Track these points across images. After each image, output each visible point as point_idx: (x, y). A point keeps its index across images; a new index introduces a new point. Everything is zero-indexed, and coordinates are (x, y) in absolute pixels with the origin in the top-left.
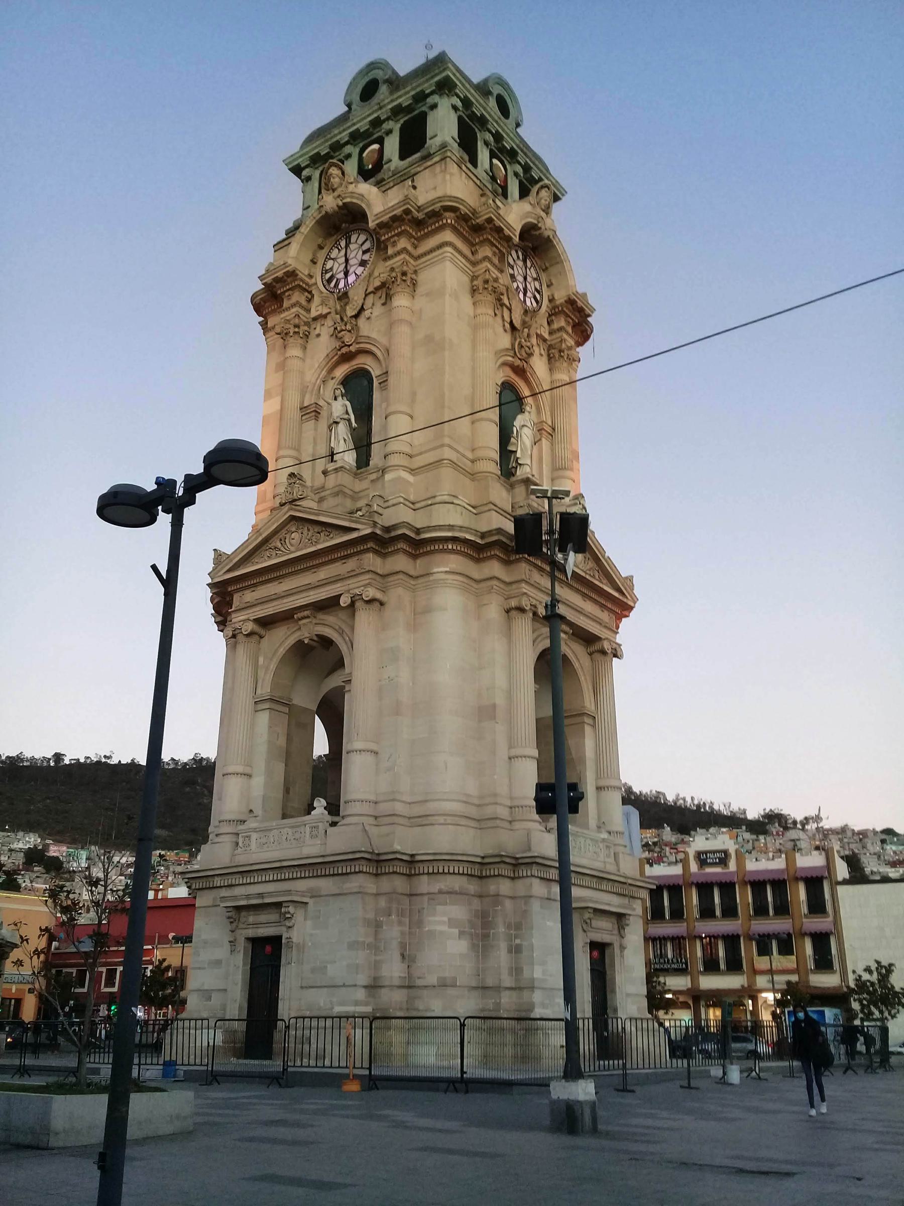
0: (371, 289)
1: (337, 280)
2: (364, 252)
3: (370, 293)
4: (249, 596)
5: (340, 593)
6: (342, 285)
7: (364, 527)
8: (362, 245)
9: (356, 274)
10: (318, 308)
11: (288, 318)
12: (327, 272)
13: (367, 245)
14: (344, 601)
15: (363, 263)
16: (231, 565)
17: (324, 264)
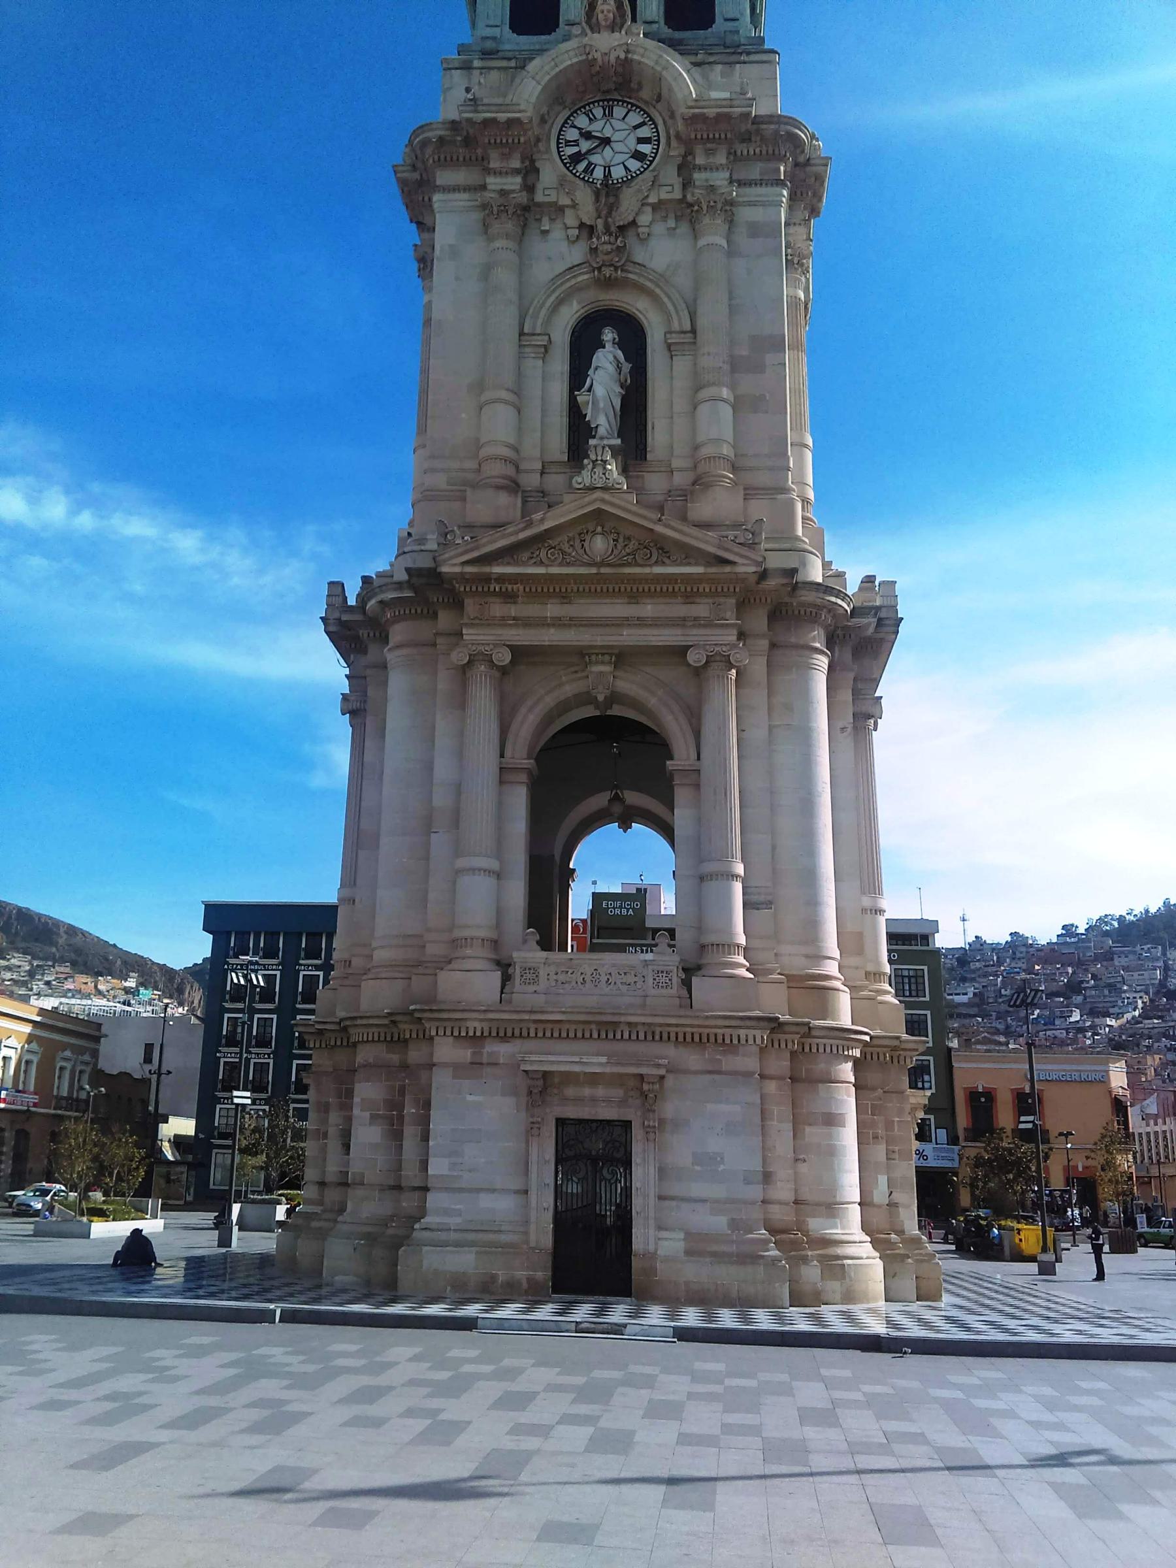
0: (651, 200)
1: (590, 164)
2: (641, 141)
3: (648, 204)
4: (498, 609)
5: (691, 644)
6: (599, 173)
8: (636, 127)
9: (626, 168)
13: (645, 132)
14: (693, 658)
15: (638, 156)
16: (475, 554)
17: (561, 130)
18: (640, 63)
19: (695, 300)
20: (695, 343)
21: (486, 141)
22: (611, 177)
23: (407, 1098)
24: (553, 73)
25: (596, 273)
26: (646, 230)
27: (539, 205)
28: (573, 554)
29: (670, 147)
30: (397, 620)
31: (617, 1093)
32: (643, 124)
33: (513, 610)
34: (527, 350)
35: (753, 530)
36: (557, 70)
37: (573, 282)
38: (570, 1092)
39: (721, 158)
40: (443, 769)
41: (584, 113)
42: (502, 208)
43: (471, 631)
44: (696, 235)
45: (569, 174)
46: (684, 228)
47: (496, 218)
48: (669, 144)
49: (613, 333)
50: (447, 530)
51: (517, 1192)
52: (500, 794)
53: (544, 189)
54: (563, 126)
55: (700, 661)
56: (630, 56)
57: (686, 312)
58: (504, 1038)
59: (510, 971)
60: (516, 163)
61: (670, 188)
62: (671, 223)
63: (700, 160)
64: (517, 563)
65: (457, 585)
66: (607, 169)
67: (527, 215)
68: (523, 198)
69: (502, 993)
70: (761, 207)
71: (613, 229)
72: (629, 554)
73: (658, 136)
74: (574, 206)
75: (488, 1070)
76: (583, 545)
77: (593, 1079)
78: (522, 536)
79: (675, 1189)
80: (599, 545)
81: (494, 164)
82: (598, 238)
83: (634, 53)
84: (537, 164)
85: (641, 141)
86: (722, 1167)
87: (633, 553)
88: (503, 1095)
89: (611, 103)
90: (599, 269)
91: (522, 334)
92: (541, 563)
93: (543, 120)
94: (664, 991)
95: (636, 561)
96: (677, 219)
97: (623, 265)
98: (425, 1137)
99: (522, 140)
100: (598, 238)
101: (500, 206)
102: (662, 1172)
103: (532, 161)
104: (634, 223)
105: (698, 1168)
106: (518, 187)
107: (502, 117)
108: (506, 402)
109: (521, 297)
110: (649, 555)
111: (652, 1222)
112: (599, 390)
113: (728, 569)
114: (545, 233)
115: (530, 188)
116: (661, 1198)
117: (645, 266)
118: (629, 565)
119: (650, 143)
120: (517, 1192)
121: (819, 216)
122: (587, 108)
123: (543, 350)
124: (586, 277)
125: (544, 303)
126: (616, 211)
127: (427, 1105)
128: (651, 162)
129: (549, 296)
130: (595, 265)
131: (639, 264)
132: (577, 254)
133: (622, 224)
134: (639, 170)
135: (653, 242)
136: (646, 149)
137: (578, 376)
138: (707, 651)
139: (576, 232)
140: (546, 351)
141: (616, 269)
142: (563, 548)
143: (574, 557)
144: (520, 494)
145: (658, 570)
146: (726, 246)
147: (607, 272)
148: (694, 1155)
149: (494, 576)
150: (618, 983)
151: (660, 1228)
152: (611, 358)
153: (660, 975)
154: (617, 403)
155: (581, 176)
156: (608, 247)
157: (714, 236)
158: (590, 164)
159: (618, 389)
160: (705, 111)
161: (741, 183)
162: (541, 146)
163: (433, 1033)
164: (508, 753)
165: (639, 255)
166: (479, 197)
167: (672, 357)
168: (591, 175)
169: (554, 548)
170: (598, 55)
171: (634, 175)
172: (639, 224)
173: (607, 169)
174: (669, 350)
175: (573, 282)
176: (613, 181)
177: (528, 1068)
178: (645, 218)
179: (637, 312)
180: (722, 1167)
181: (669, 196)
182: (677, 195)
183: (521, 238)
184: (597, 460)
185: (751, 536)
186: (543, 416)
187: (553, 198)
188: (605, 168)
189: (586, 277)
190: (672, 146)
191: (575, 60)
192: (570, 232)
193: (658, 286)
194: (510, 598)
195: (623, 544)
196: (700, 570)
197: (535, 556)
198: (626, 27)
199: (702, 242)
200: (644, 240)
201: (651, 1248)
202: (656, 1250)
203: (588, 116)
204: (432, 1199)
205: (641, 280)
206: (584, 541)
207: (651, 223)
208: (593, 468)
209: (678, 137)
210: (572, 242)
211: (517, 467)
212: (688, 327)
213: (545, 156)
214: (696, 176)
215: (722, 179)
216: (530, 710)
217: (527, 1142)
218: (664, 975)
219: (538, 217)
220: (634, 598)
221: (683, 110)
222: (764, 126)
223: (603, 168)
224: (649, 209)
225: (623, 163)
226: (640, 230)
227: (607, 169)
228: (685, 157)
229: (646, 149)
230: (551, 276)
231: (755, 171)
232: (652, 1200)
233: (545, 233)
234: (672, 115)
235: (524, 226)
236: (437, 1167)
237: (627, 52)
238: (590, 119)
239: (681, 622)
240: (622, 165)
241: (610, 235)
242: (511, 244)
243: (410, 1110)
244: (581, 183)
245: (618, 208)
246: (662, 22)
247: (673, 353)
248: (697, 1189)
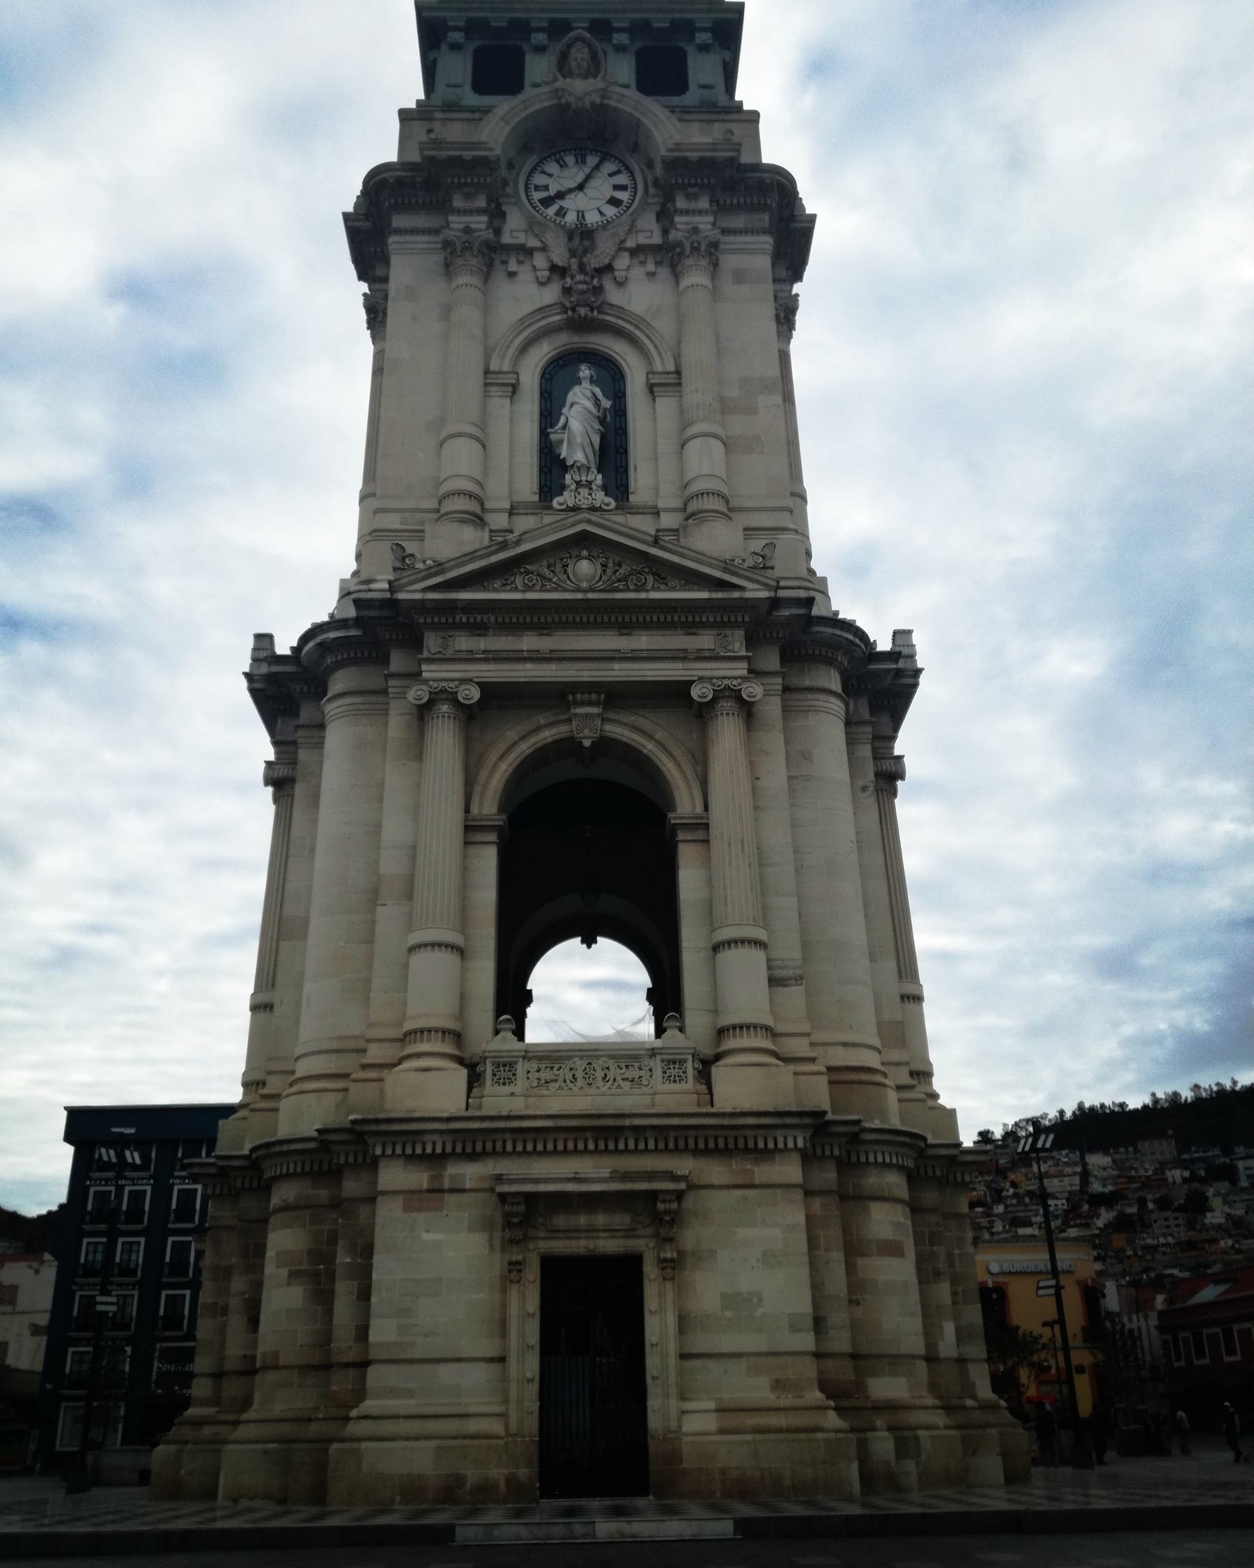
0: (630, 243)
1: (561, 208)
2: (616, 188)
3: (626, 249)
4: (463, 642)
6: (571, 218)
7: (757, 586)
8: (611, 175)
9: (601, 213)
10: (515, 234)
11: (473, 226)
12: (537, 188)
15: (614, 202)
18: (616, 109)
19: (679, 343)
20: (680, 384)
21: (449, 181)
23: (341, 1242)
24: (523, 115)
25: (570, 312)
26: (623, 274)
27: (509, 249)
28: (554, 580)
29: (647, 195)
30: (339, 665)
31: (621, 1220)
32: (618, 172)
33: (482, 644)
34: (493, 389)
35: (762, 553)
36: (528, 112)
37: (543, 323)
38: (561, 1221)
39: (704, 203)
40: (395, 830)
41: (555, 160)
42: (467, 245)
43: (433, 667)
44: (677, 277)
45: (540, 216)
46: (664, 272)
47: (460, 256)
48: (646, 191)
49: (590, 369)
50: (405, 554)
51: (491, 1360)
52: (465, 856)
53: (511, 231)
55: (707, 696)
56: (606, 102)
57: (669, 354)
58: (473, 1157)
59: (479, 1069)
60: (481, 202)
61: (649, 234)
62: (651, 267)
63: (681, 203)
64: (486, 589)
65: (416, 617)
66: (581, 215)
67: (493, 255)
68: (489, 235)
69: (468, 1097)
70: (747, 256)
71: (588, 269)
72: (619, 580)
73: (635, 183)
74: (544, 249)
75: (449, 1198)
76: (566, 571)
77: (592, 1201)
78: (494, 559)
79: (701, 1343)
80: (585, 567)
81: (458, 202)
82: (572, 277)
83: (610, 98)
84: (504, 208)
85: (616, 188)
86: (760, 1312)
87: (624, 579)
88: (471, 1229)
89: (583, 152)
90: (573, 309)
91: (487, 372)
92: (516, 590)
93: (511, 166)
94: (677, 1087)
95: (628, 587)
96: (658, 263)
97: (600, 306)
98: (365, 1294)
99: (489, 180)
100: (572, 277)
101: (464, 243)
102: (684, 1323)
103: (499, 205)
104: (609, 268)
105: (728, 1314)
106: (483, 226)
107: (468, 154)
108: (471, 436)
109: (486, 336)
110: (643, 581)
111: (673, 1391)
112: (576, 425)
113: (736, 595)
114: (512, 275)
115: (498, 232)
116: (684, 1356)
117: (623, 308)
118: (617, 590)
120: (491, 1360)
121: (802, 281)
122: (558, 156)
123: (510, 389)
124: (558, 318)
125: (512, 342)
126: (591, 253)
127: (368, 1251)
128: (628, 208)
129: (517, 335)
130: (568, 304)
131: (616, 306)
132: (551, 294)
133: (597, 266)
134: (615, 215)
135: (632, 286)
136: (624, 196)
137: (549, 413)
138: (714, 685)
139: (546, 274)
140: (514, 392)
141: (592, 309)
142: (542, 573)
143: (555, 583)
144: (487, 529)
145: (655, 595)
146: (710, 286)
147: (582, 311)
148: (724, 1296)
149: (459, 605)
150: (619, 1079)
151: (683, 1398)
152: (590, 395)
153: (672, 1066)
154: (596, 440)
155: (553, 220)
156: (584, 287)
157: (696, 277)
158: (561, 208)
159: (597, 426)
160: (688, 154)
161: (725, 231)
162: (509, 190)
163: (378, 1151)
164: (475, 810)
165: (614, 295)
166: (439, 238)
167: (654, 400)
169: (533, 574)
170: (572, 100)
171: (610, 220)
172: (616, 268)
174: (652, 392)
175: (543, 323)
177: (506, 1188)
178: (622, 262)
179: (614, 355)
180: (760, 1312)
181: (648, 242)
182: (657, 239)
183: (487, 274)
184: (581, 481)
185: (761, 559)
186: (511, 457)
187: (521, 239)
188: (578, 212)
189: (558, 318)
190: (650, 194)
191: (546, 104)
192: (539, 274)
193: (637, 327)
194: (479, 629)
195: (612, 570)
196: (705, 595)
197: (509, 582)
198: (600, 75)
199: (685, 283)
200: (620, 284)
201: (673, 1424)
202: (680, 1427)
203: (558, 162)
204: (374, 1375)
205: (620, 322)
206: (567, 566)
207: (629, 267)
208: (577, 488)
209: (656, 183)
210: (542, 284)
211: (482, 504)
212: (671, 367)
213: (512, 200)
214: (677, 219)
215: (706, 223)
216: (502, 757)
217: (504, 1291)
218: (677, 1066)
219: (504, 258)
220: (626, 628)
221: (663, 152)
222: (749, 175)
224: (626, 255)
226: (617, 273)
227: (580, 214)
228: (663, 205)
229: (624, 196)
230: (519, 317)
231: (739, 221)
232: (673, 1361)
233: (512, 275)
234: (650, 165)
235: (490, 266)
236: (382, 1332)
237: (603, 97)
238: (561, 166)
239: (682, 656)
241: (586, 274)
242: (475, 280)
243: (344, 1258)
244: (553, 225)
245: (593, 250)
246: (634, 86)
247: (656, 394)
248: (727, 1343)
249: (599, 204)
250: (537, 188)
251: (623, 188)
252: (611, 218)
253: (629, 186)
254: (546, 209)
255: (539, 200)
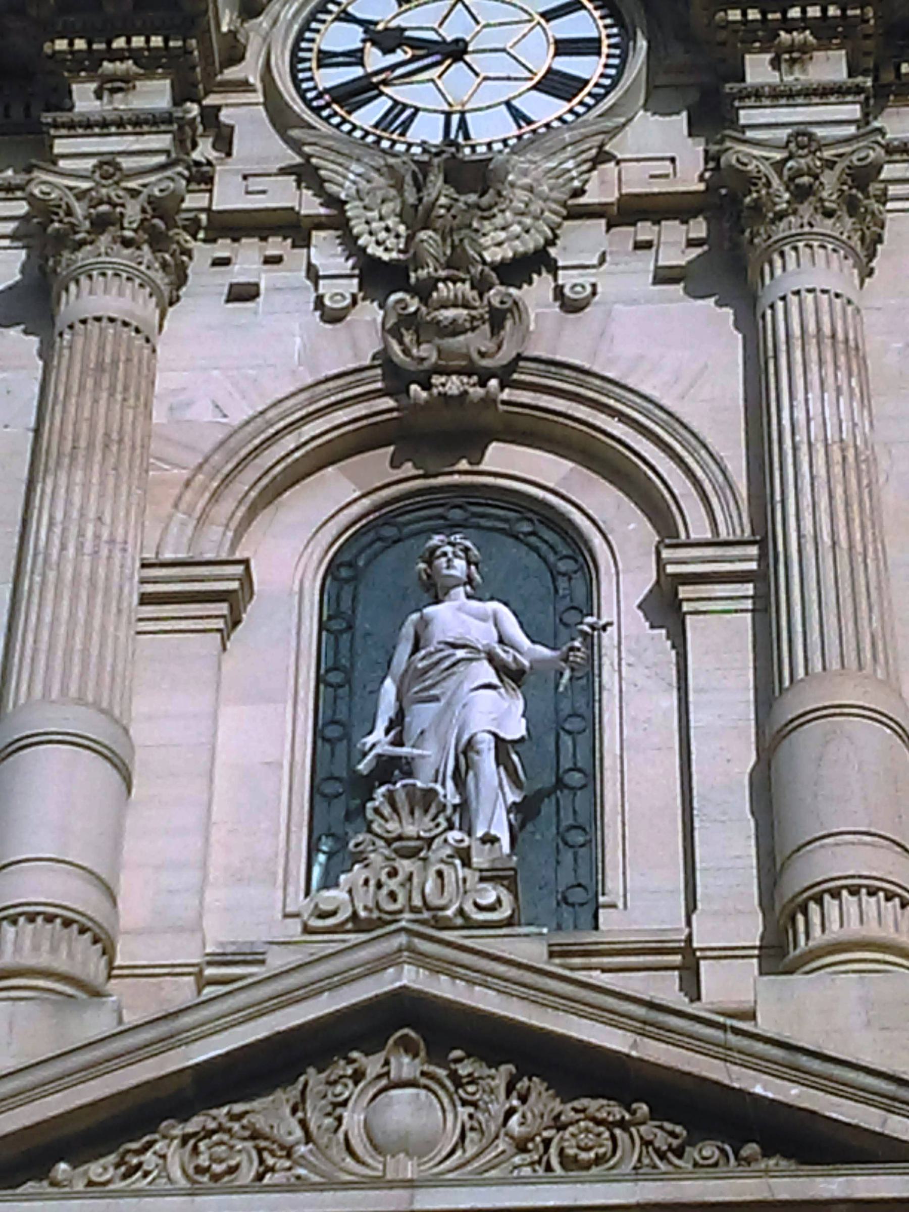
9: (518, 116)
22: (467, 137)
54: (313, 17)
119: (599, 54)
168: (402, 134)
173: (455, 119)
176: (473, 147)
188: (448, 115)
223: (442, 117)
225: (508, 104)
227: (455, 119)
240: (503, 108)
249: (508, 90)
250: (326, 59)
251: (589, 47)
252: (547, 126)
253: (605, 42)
254: (349, 113)
255: (327, 91)
